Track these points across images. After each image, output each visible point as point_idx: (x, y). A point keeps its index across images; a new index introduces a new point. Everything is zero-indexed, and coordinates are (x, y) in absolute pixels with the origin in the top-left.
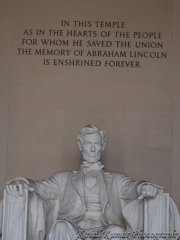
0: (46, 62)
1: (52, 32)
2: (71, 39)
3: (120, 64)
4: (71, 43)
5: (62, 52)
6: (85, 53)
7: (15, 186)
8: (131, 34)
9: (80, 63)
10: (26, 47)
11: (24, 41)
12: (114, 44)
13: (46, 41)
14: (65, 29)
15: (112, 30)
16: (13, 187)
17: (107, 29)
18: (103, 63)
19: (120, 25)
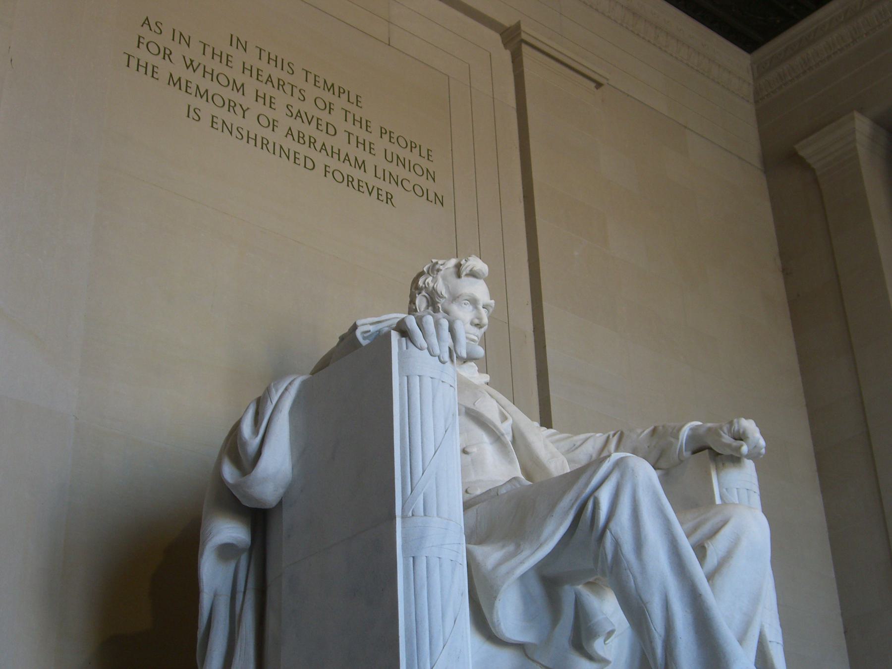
0: (193, 114)
1: (209, 51)
2: (251, 85)
3: (355, 184)
4: (250, 91)
5: (231, 106)
6: (281, 130)
7: (445, 324)
8: (375, 128)
9: (271, 147)
10: (143, 54)
11: (141, 40)
12: (342, 136)
13: (195, 64)
14: (238, 56)
15: (340, 103)
16: (437, 324)
17: (328, 97)
18: (320, 168)
19: (353, 99)
